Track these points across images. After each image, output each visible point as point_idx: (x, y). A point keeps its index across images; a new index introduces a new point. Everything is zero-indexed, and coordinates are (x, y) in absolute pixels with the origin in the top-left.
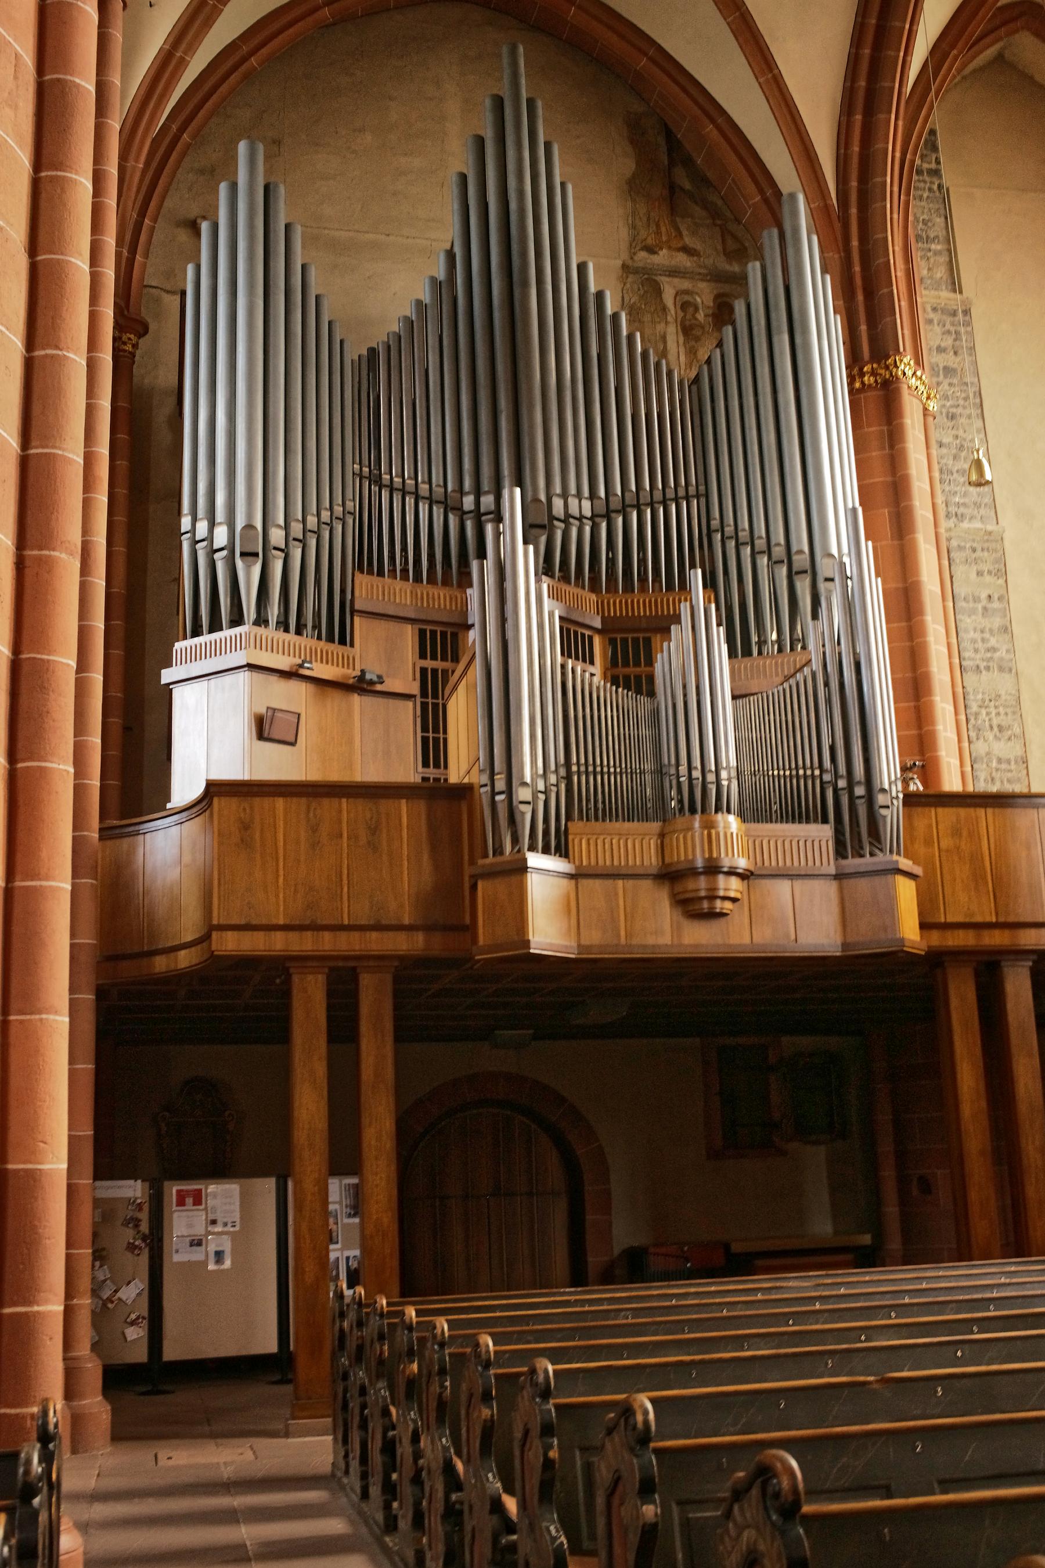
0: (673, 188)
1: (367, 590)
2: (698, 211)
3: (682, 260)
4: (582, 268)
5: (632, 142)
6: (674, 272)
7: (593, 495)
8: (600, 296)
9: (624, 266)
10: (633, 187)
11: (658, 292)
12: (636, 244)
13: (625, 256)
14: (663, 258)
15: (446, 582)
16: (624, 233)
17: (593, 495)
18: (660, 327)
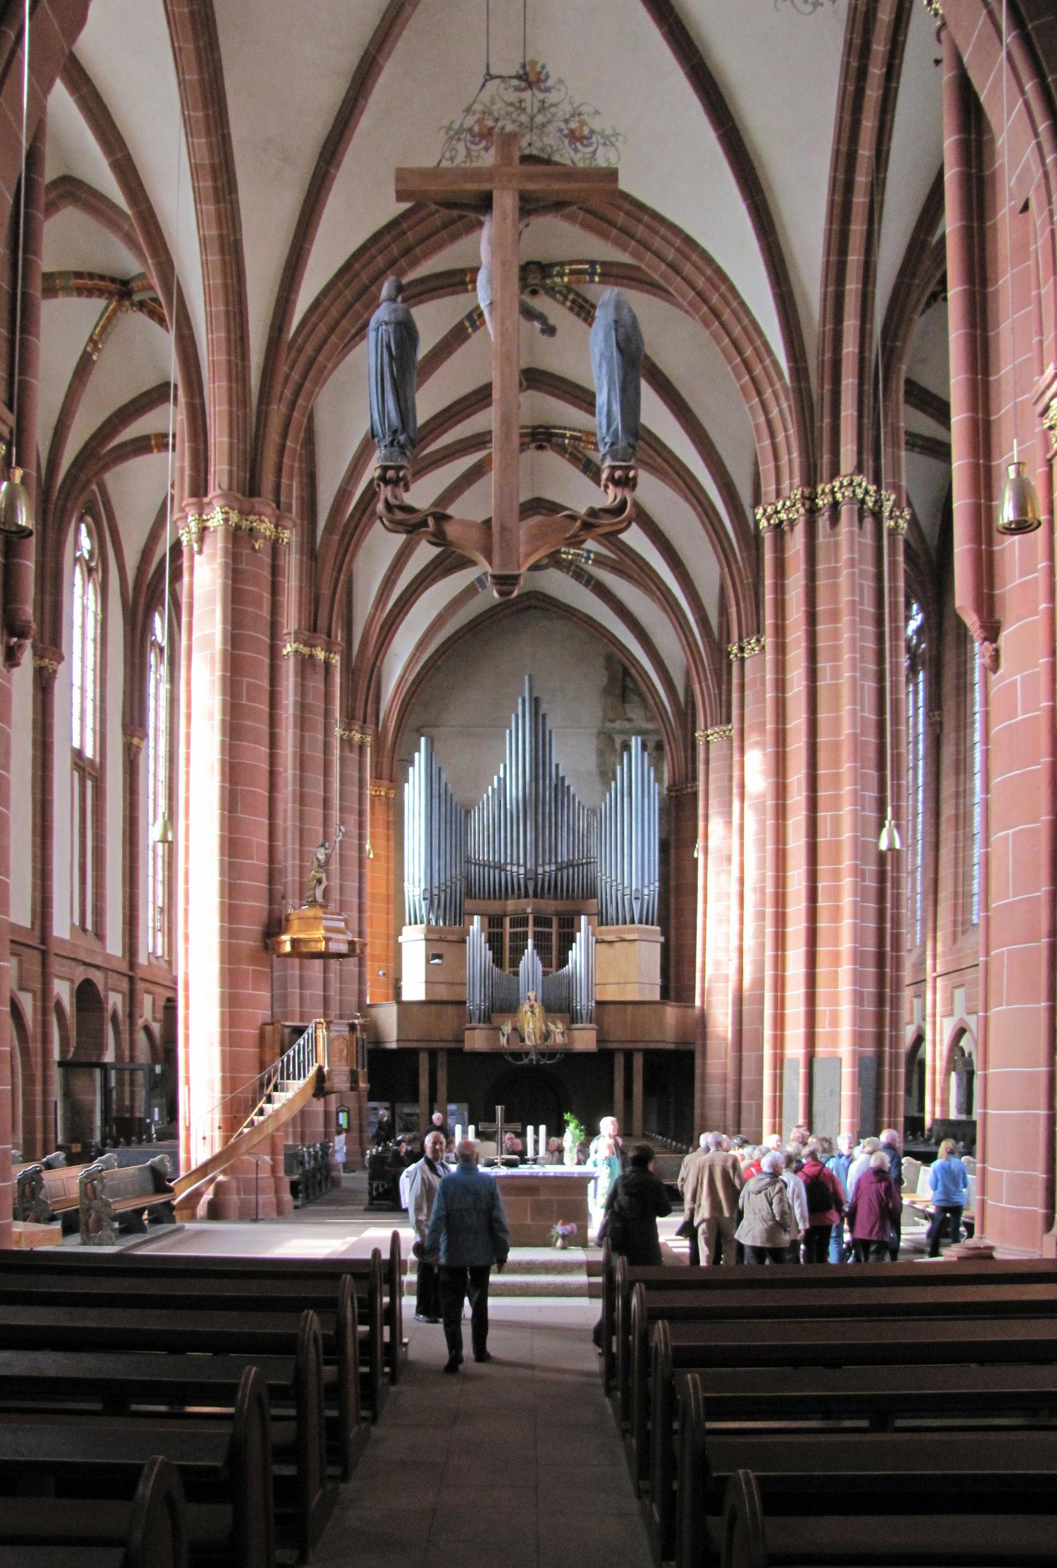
0: (624, 689)
1: (469, 904)
2: (636, 699)
3: (627, 725)
4: (557, 766)
5: (607, 669)
6: (621, 732)
7: (556, 862)
8: (563, 778)
9: (599, 733)
10: (607, 691)
11: (613, 741)
12: (604, 720)
13: (599, 725)
14: (618, 725)
15: (500, 898)
16: (600, 714)
17: (556, 862)
18: (613, 759)
